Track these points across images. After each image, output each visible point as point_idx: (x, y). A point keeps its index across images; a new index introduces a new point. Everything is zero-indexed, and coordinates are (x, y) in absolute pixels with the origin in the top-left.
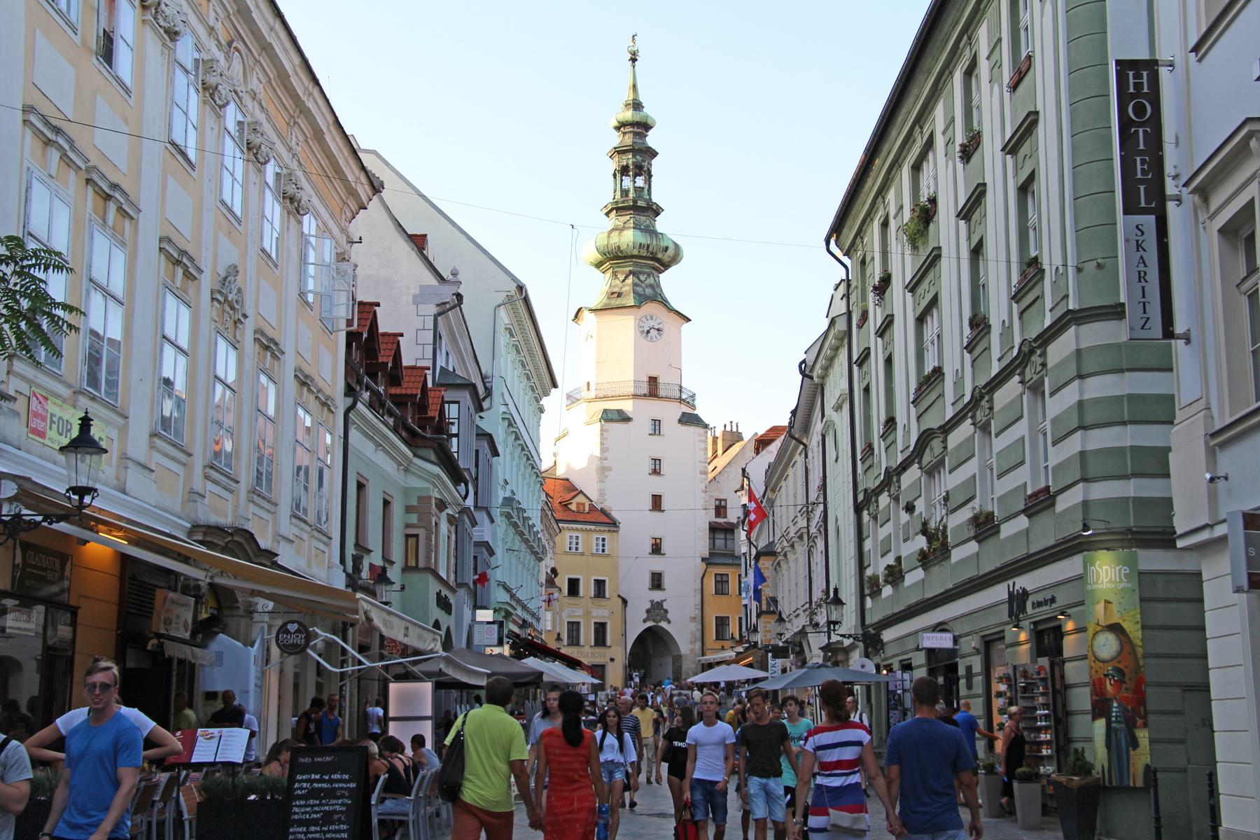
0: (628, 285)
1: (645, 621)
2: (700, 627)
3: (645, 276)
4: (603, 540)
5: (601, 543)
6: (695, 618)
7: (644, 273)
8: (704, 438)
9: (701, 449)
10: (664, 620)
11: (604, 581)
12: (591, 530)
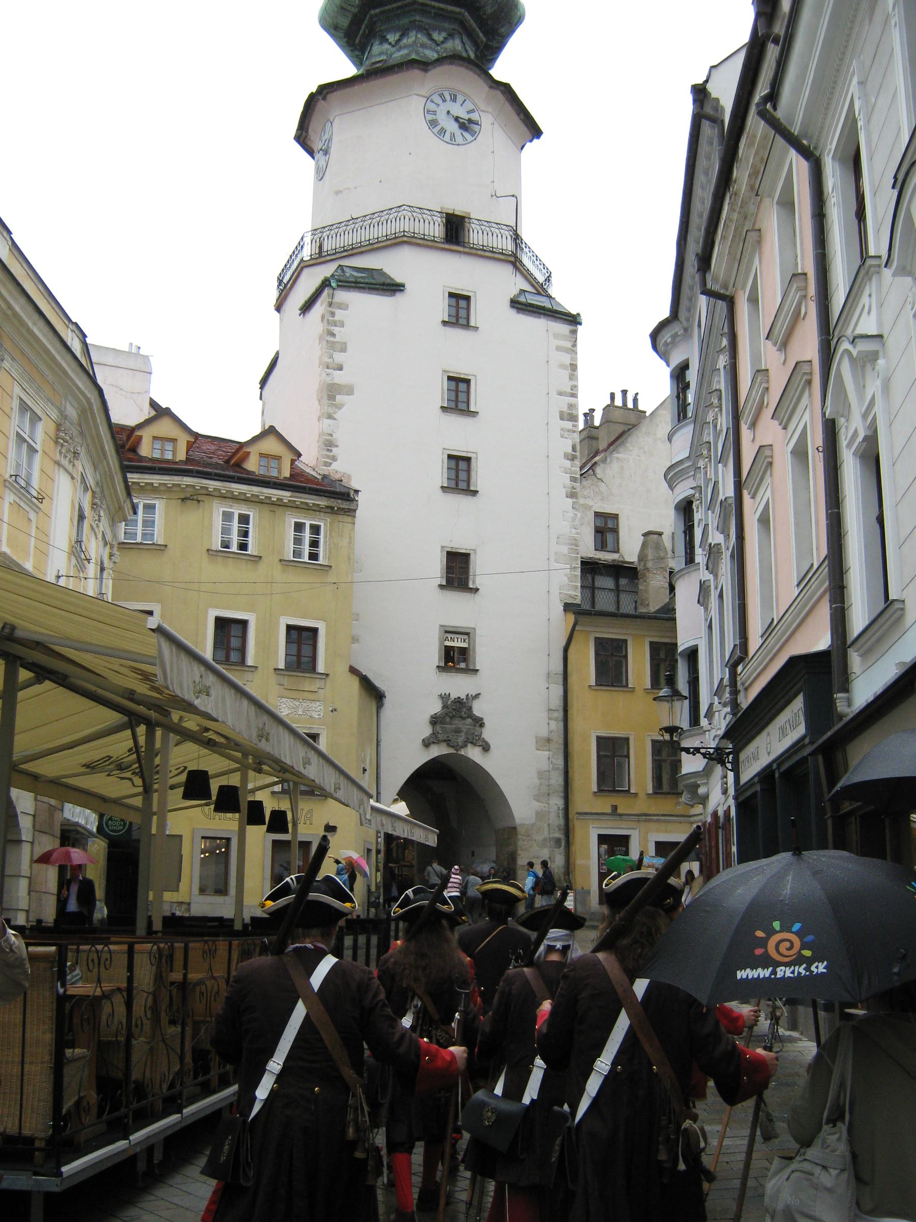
0: (405, 47)
1: (427, 744)
2: (560, 762)
3: (444, 34)
4: (315, 529)
5: (307, 535)
6: (549, 740)
7: (441, 30)
8: (569, 345)
9: (562, 366)
10: (475, 744)
11: (315, 631)
12: (279, 504)
